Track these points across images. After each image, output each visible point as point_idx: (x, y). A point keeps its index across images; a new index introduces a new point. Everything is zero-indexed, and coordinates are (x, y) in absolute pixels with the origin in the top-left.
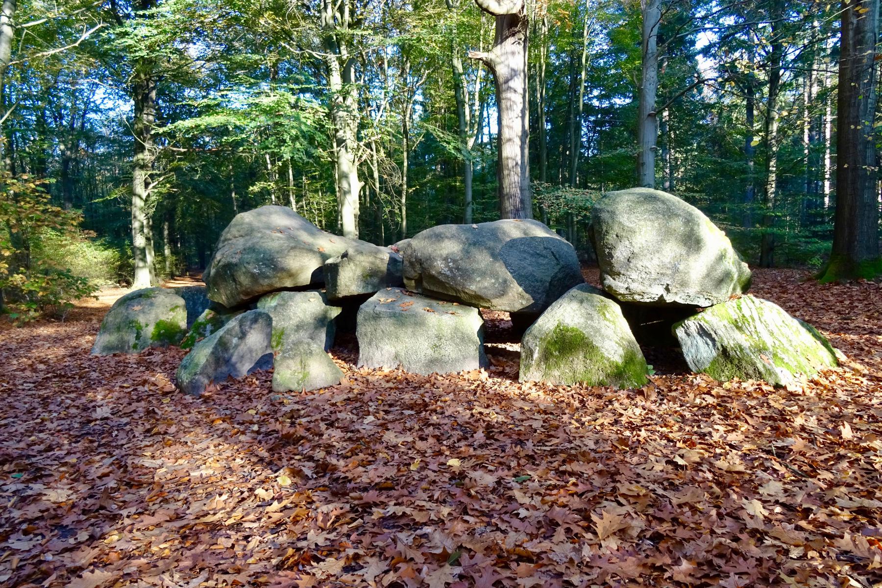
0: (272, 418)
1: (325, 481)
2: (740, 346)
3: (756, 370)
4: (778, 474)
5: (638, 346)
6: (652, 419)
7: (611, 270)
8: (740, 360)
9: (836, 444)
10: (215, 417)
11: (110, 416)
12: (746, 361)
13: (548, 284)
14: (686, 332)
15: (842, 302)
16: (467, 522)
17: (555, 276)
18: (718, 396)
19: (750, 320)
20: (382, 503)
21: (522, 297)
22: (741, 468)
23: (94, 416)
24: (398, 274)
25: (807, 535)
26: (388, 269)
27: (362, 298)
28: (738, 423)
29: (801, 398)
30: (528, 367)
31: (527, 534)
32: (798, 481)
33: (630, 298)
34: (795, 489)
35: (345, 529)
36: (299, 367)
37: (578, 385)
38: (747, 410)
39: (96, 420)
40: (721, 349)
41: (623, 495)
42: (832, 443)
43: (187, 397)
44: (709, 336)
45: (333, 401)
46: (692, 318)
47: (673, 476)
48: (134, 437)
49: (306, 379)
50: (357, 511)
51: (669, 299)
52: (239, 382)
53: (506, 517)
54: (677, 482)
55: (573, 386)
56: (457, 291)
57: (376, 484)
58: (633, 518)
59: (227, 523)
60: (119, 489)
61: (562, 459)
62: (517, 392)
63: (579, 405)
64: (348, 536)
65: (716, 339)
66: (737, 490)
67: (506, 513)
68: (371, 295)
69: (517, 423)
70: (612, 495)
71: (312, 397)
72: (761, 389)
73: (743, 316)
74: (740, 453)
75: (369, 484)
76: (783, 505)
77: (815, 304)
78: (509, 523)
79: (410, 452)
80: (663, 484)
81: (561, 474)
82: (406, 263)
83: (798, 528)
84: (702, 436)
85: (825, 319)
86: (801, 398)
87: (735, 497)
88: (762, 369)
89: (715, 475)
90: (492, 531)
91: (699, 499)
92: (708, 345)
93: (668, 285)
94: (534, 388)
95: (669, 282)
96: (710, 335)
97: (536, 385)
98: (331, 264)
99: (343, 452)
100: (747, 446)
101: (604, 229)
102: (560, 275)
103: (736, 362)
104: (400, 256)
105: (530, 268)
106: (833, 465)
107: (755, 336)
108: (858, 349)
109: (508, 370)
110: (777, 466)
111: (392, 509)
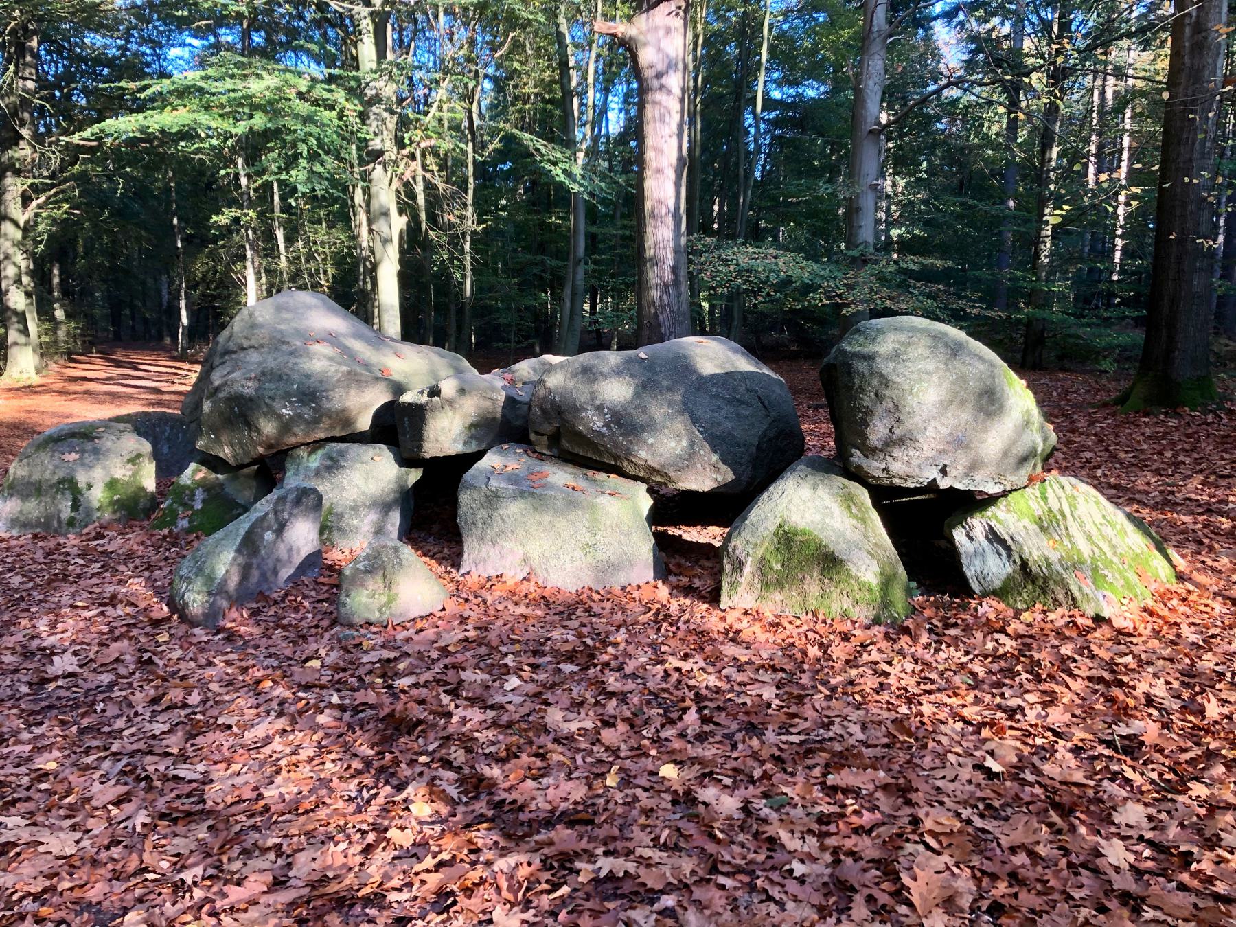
0: (352, 675)
1: (481, 807)
2: (1047, 559)
3: (1068, 593)
4: (1132, 786)
5: (889, 541)
6: (933, 682)
7: (863, 444)
8: (1046, 579)
9: (1200, 729)
10: (259, 674)
11: (78, 669)
12: (1055, 582)
13: (754, 449)
14: (968, 535)
15: (1160, 453)
16: (722, 887)
17: (764, 435)
18: (1018, 637)
19: (1059, 517)
20: (585, 851)
21: (718, 470)
22: (1078, 777)
23: (52, 670)
24: (518, 423)
25: (1193, 899)
26: (503, 415)
27: (467, 461)
28: (1058, 689)
29: (1135, 640)
30: (734, 586)
31: (813, 906)
32: (1165, 799)
33: (886, 482)
34: (1163, 816)
35: (545, 901)
36: (382, 585)
37: (810, 614)
38: (1064, 663)
39: (56, 678)
40: (1019, 562)
41: (931, 833)
42: (1195, 727)
43: (197, 631)
44: (1002, 542)
45: (442, 644)
46: (978, 515)
47: (988, 793)
48: (136, 714)
49: (393, 605)
50: (552, 867)
51: (944, 484)
52: (276, 602)
53: (775, 876)
54: (997, 804)
55: (804, 617)
56: (616, 458)
57: (563, 813)
58: (953, 874)
59: (360, 894)
60: (156, 826)
61: (822, 762)
62: (721, 626)
63: (819, 654)
64: (554, 914)
65: (1013, 547)
66: (1083, 817)
67: (774, 868)
68: (479, 455)
69: (736, 688)
70: (914, 832)
71: (405, 634)
72: (1075, 624)
73: (1050, 510)
74: (1069, 745)
75: (552, 812)
76: (1151, 843)
77: (1122, 455)
78: (783, 886)
79: (595, 749)
80: (977, 807)
81: (831, 791)
82: (536, 410)
83: (1182, 887)
84: (1011, 713)
85: (1140, 484)
86: (1135, 640)
87: (1083, 830)
88: (1077, 594)
89: (1047, 791)
90: (762, 901)
91: (1036, 838)
92: (1000, 555)
93: (945, 466)
94: (745, 620)
95: (946, 462)
96: (1005, 541)
97: (746, 613)
98: (410, 404)
99: (493, 749)
100: (1079, 734)
101: (857, 383)
102: (771, 434)
103: (1041, 582)
104: (522, 394)
105: (728, 424)
106: (1203, 769)
107: (1066, 542)
108: (1195, 541)
109: (697, 583)
110: (1129, 773)
111: (606, 865)
